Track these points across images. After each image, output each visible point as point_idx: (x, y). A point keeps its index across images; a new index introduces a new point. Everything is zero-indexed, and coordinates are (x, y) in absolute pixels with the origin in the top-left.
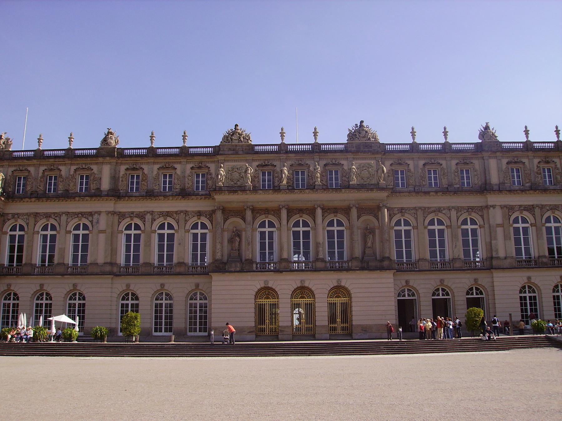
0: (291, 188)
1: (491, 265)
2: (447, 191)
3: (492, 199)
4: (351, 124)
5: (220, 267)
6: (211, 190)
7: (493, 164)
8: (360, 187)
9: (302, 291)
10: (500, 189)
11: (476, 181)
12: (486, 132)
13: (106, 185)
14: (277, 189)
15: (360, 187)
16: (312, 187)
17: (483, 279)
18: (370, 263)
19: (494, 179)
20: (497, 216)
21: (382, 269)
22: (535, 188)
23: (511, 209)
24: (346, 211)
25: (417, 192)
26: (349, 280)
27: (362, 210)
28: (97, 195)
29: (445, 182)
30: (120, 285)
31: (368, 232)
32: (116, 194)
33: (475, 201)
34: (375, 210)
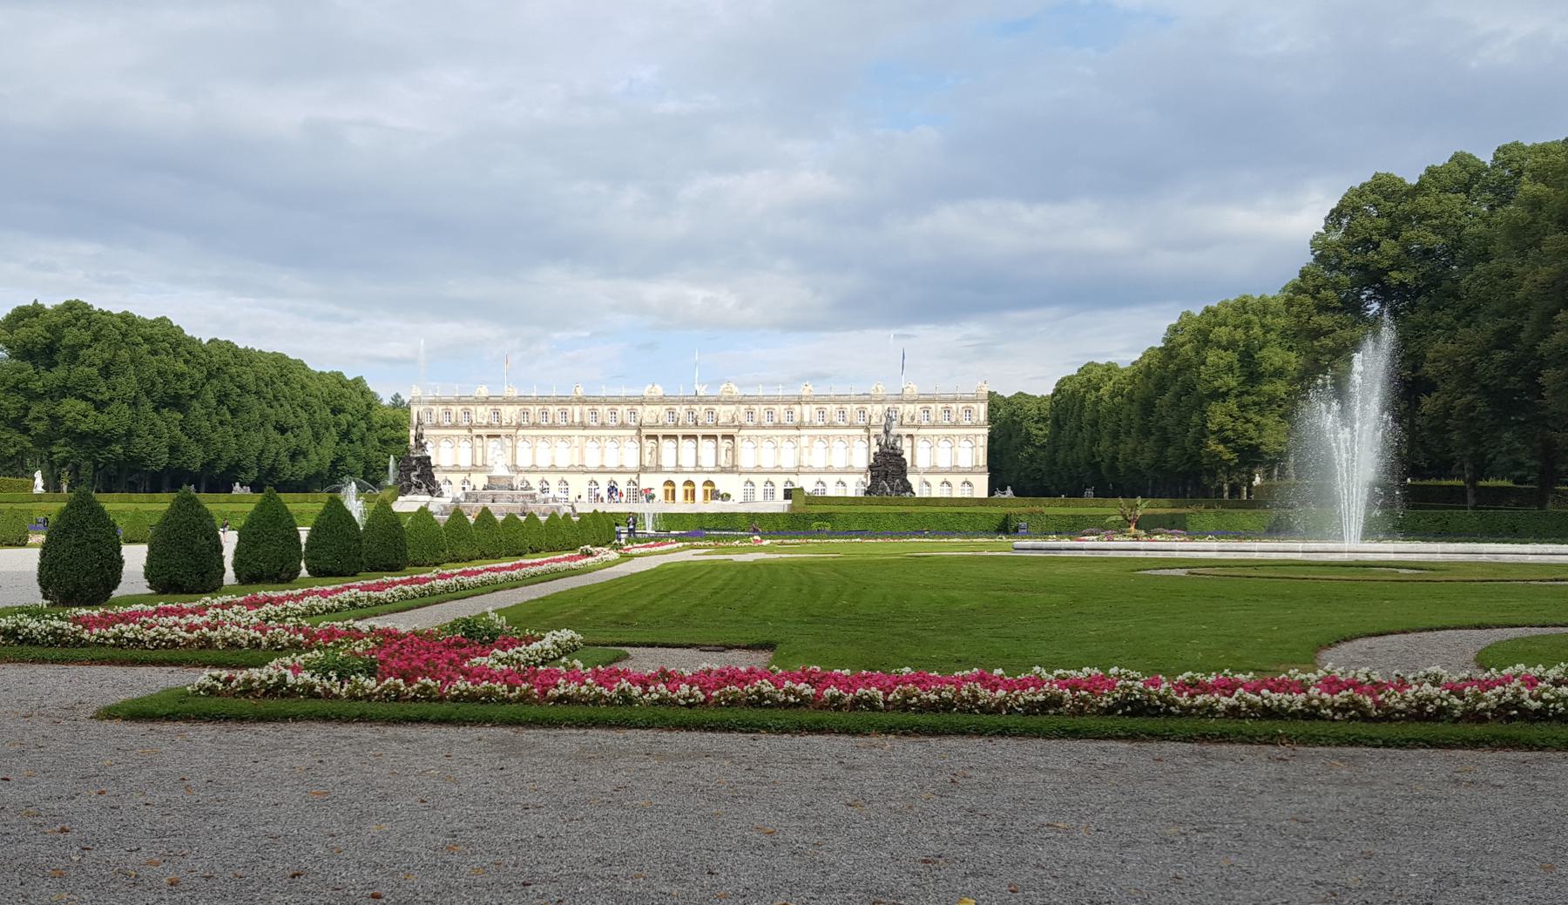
2: (775, 427)
3: (803, 432)
5: (643, 469)
7: (806, 408)
11: (797, 419)
13: (577, 419)
19: (806, 419)
21: (732, 472)
23: (814, 437)
27: (724, 437)
28: (572, 426)
29: (776, 420)
30: (589, 477)
32: (583, 426)
33: (796, 432)
34: (731, 437)
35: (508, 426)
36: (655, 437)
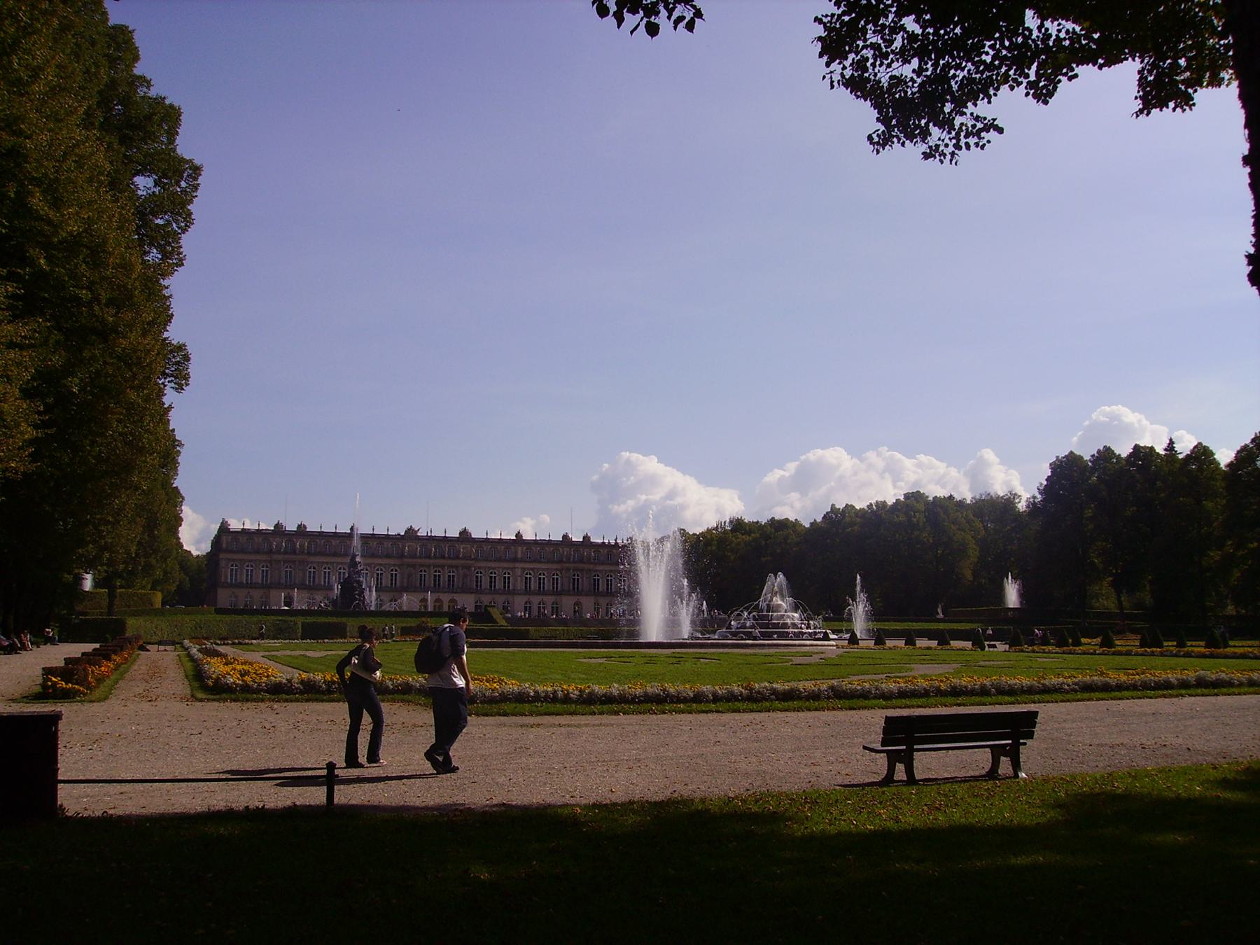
0: (435, 557)
1: (514, 592)
3: (517, 565)
4: (461, 529)
6: (402, 556)
8: (464, 558)
9: (438, 600)
10: (521, 561)
12: (518, 535)
14: (429, 557)
15: (464, 558)
16: (443, 557)
17: (510, 598)
18: (465, 590)
20: (519, 572)
22: (535, 561)
23: (524, 569)
24: (457, 567)
25: (486, 560)
26: (456, 597)
27: (464, 567)
31: (465, 576)
34: (468, 568)
35: (302, 552)
36: (414, 566)
